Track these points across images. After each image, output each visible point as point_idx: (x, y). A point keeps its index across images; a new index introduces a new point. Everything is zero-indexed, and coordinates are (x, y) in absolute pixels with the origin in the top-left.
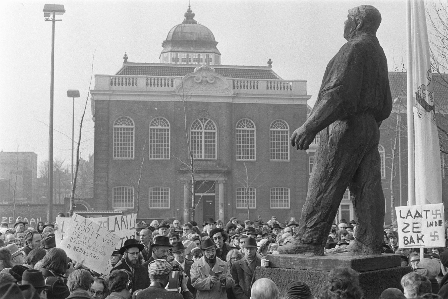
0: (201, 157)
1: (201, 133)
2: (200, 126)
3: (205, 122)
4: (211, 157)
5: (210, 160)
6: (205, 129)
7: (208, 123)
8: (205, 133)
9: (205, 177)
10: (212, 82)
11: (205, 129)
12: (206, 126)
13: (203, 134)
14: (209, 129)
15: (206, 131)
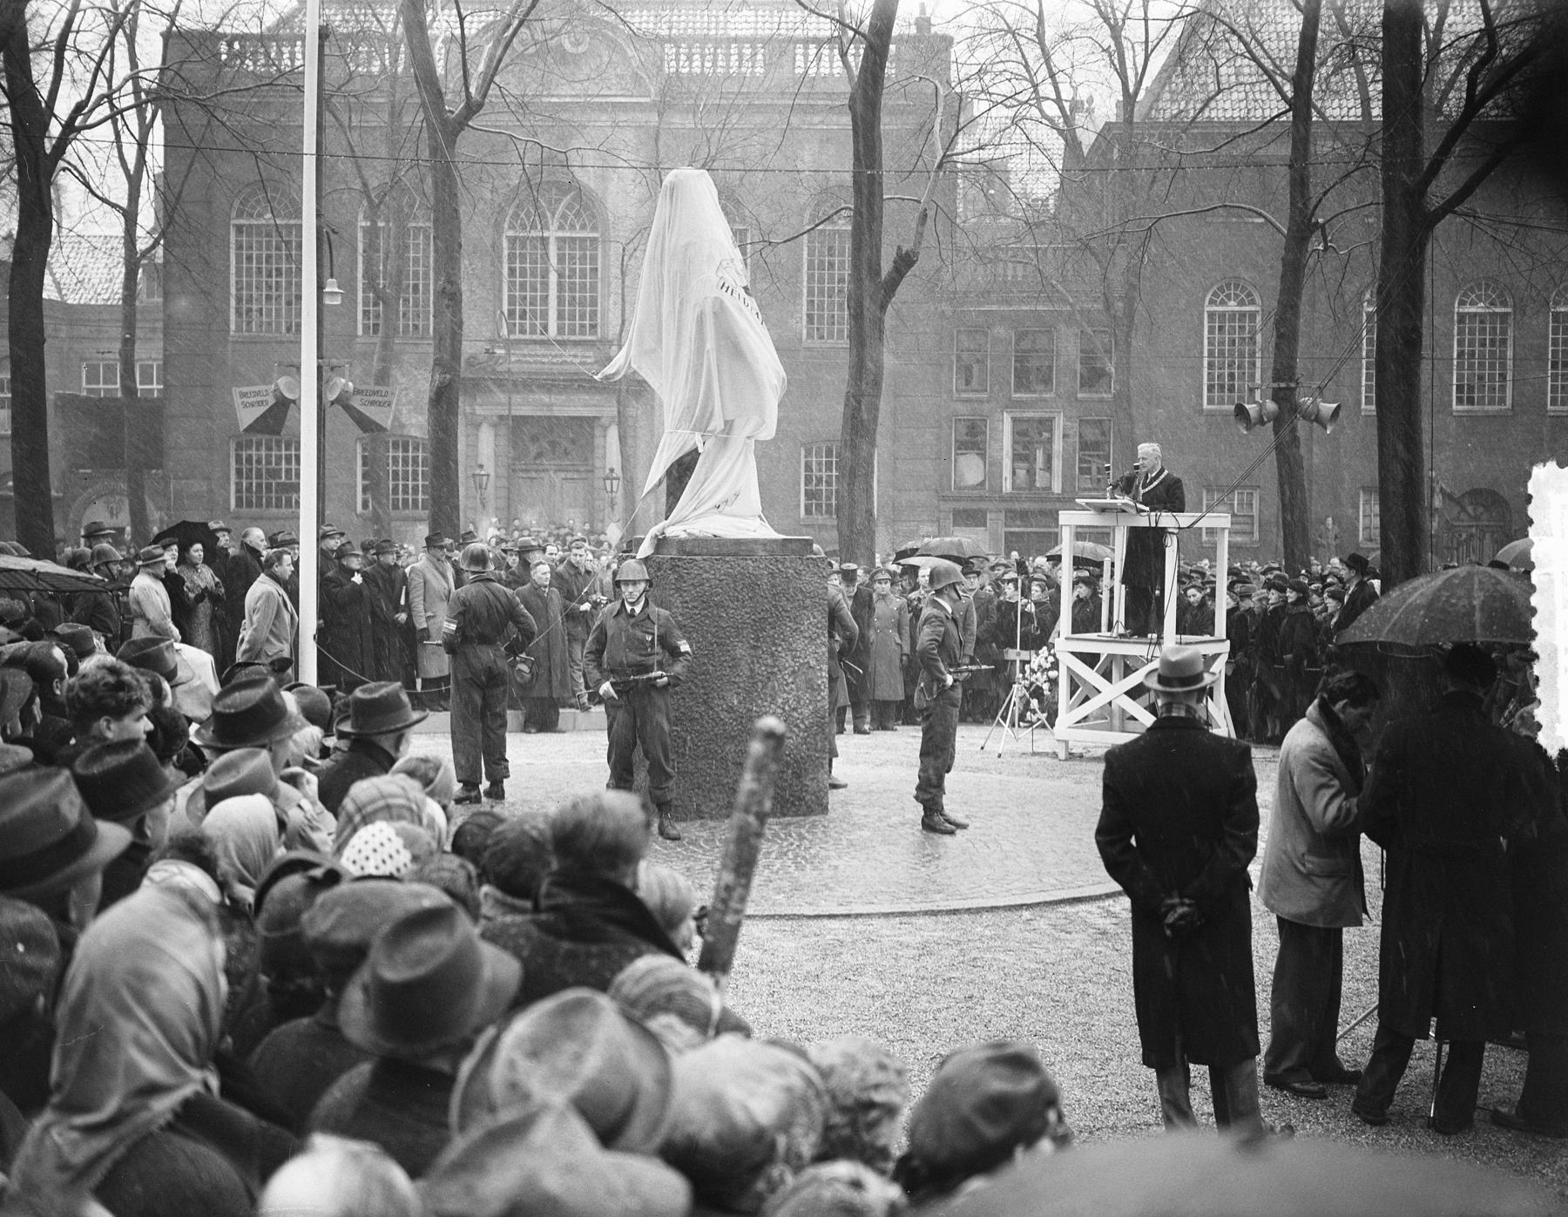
0: (545, 328)
1: (544, 241)
2: (542, 216)
3: (558, 201)
4: (582, 333)
5: (576, 343)
6: (561, 227)
7: (569, 207)
8: (561, 241)
9: (550, 406)
10: (581, 49)
11: (561, 227)
12: (564, 216)
13: (552, 240)
14: (572, 227)
15: (560, 234)
